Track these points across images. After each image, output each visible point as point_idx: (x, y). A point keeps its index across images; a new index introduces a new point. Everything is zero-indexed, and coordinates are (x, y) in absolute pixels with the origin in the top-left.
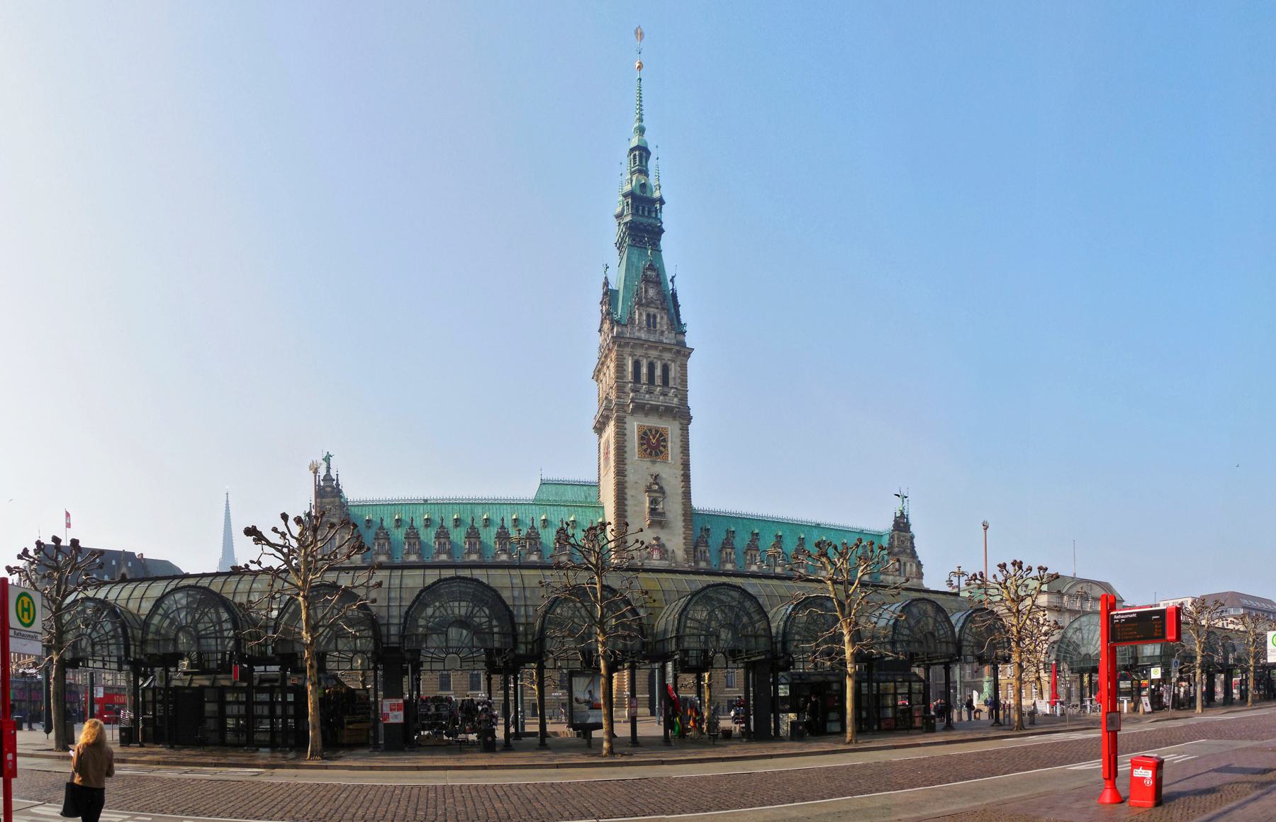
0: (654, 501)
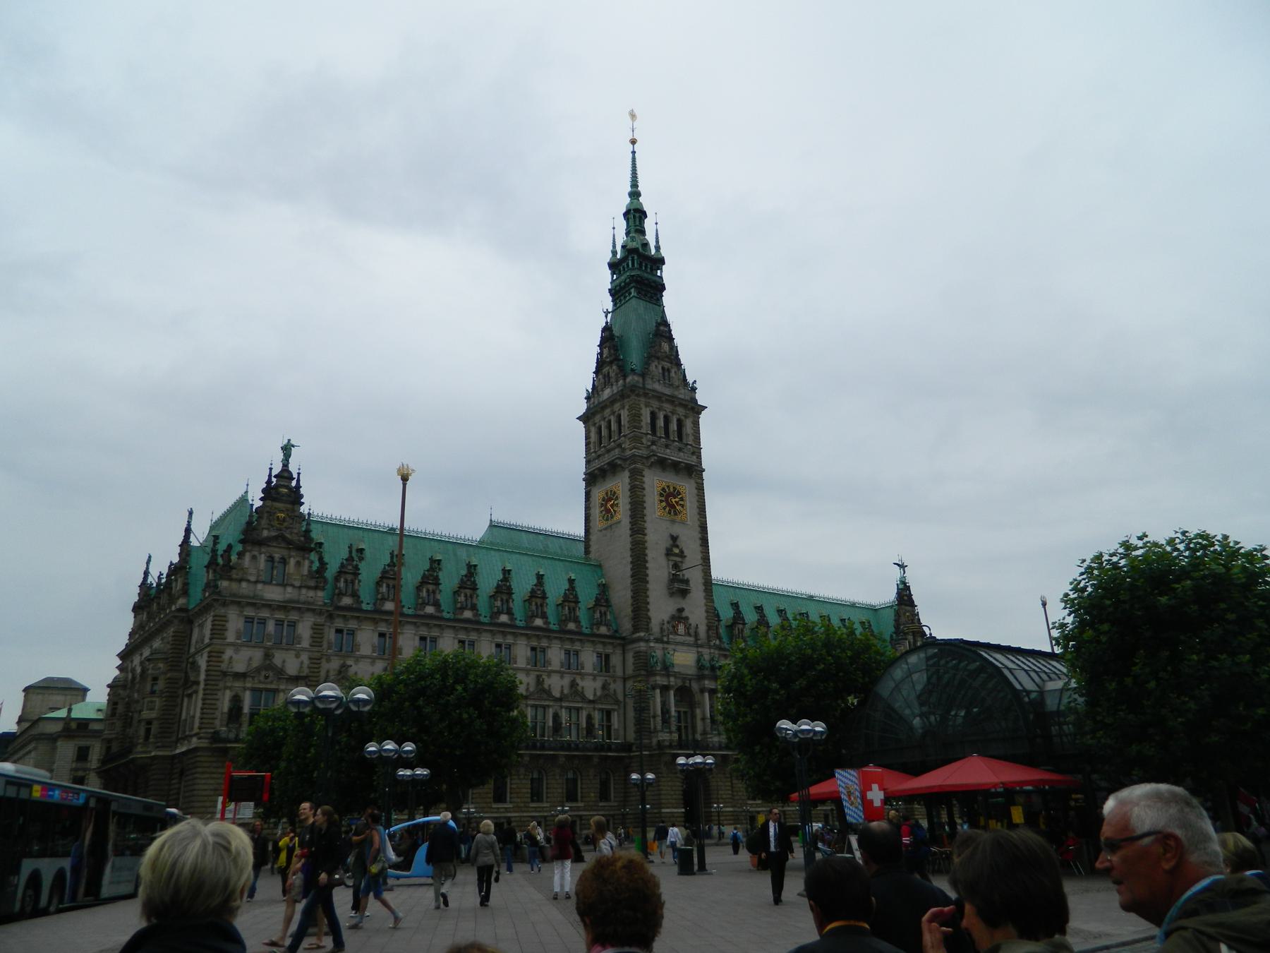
0: (676, 566)
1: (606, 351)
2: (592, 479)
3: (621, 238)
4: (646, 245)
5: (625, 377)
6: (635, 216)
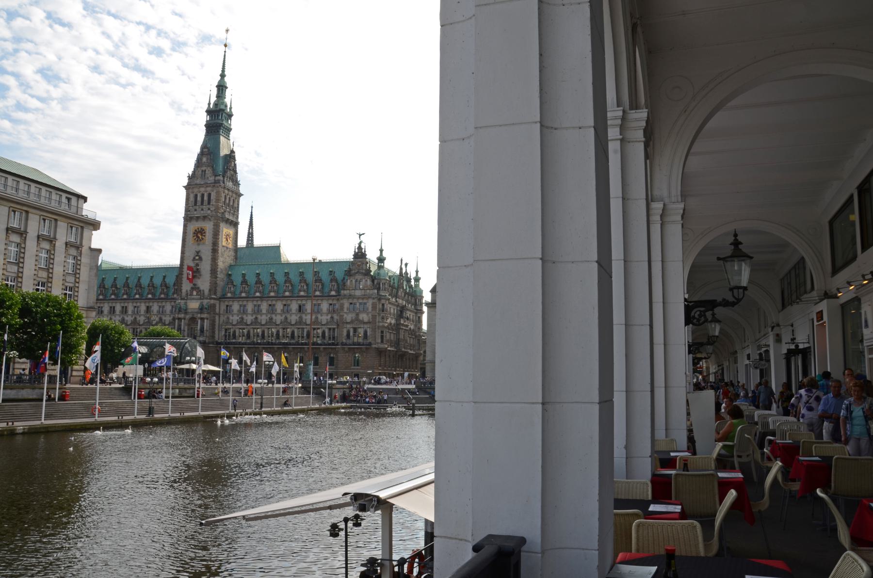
1: (204, 160)
2: (188, 219)
3: (214, 99)
4: (226, 106)
5: (216, 176)
6: (221, 88)
